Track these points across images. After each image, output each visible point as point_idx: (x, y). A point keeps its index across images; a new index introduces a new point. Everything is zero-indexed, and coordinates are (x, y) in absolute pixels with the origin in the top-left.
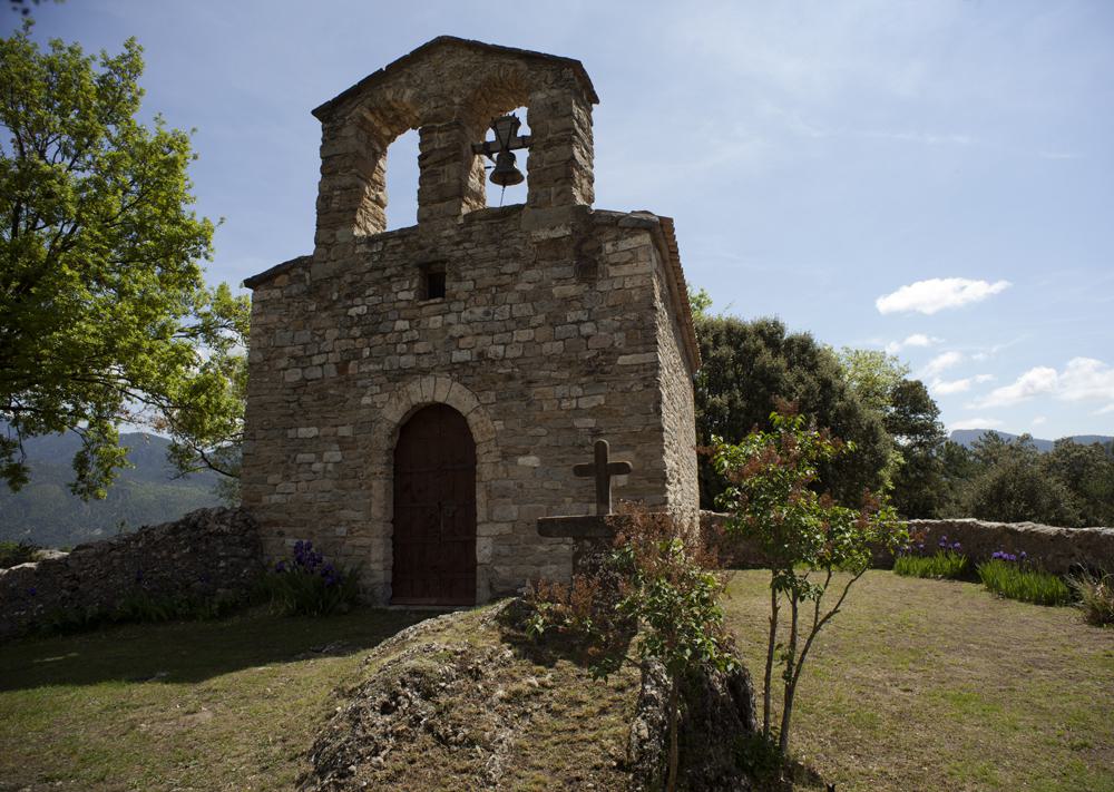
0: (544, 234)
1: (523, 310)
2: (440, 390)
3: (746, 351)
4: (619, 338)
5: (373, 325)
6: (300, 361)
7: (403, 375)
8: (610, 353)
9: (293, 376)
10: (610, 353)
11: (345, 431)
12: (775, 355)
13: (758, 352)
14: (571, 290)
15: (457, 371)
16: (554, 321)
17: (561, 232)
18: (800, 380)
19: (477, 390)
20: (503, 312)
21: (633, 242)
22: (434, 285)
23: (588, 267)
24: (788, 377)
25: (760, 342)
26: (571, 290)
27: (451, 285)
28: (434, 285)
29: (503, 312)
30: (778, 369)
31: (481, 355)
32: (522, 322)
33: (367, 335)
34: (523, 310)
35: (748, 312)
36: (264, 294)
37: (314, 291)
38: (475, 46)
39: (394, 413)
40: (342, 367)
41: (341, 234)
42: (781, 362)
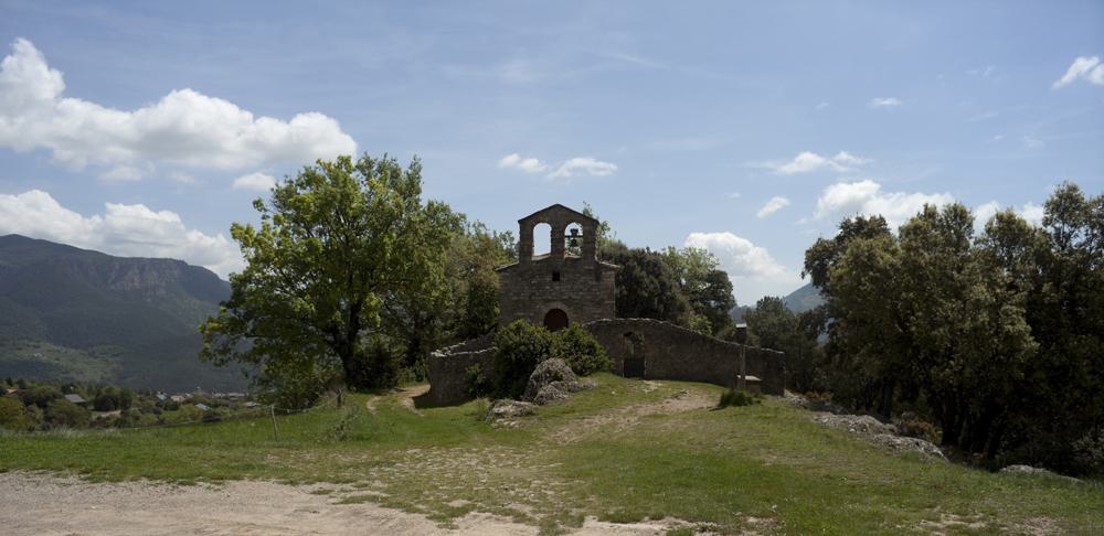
0: (587, 267)
1: (581, 287)
2: (559, 306)
3: (629, 266)
4: (606, 297)
5: (539, 286)
6: (518, 294)
7: (548, 301)
8: (603, 300)
9: (515, 298)
10: (603, 300)
11: (532, 314)
12: (642, 270)
13: (634, 268)
14: (594, 283)
15: (563, 300)
16: (589, 290)
17: (592, 268)
18: (652, 282)
19: (569, 307)
20: (576, 287)
21: (609, 273)
22: (556, 277)
23: (598, 278)
24: (647, 281)
25: (636, 263)
26: (594, 283)
27: (561, 278)
28: (556, 277)
29: (576, 287)
30: (642, 277)
31: (570, 298)
32: (581, 290)
33: (538, 289)
34: (581, 287)
35: (633, 243)
36: (503, 274)
37: (521, 275)
38: (571, 211)
39: (546, 311)
40: (530, 297)
41: (528, 259)
42: (644, 273)
